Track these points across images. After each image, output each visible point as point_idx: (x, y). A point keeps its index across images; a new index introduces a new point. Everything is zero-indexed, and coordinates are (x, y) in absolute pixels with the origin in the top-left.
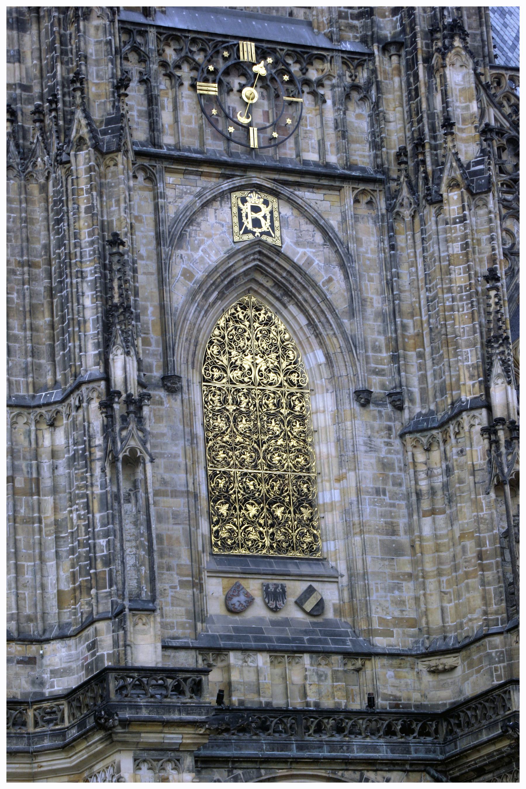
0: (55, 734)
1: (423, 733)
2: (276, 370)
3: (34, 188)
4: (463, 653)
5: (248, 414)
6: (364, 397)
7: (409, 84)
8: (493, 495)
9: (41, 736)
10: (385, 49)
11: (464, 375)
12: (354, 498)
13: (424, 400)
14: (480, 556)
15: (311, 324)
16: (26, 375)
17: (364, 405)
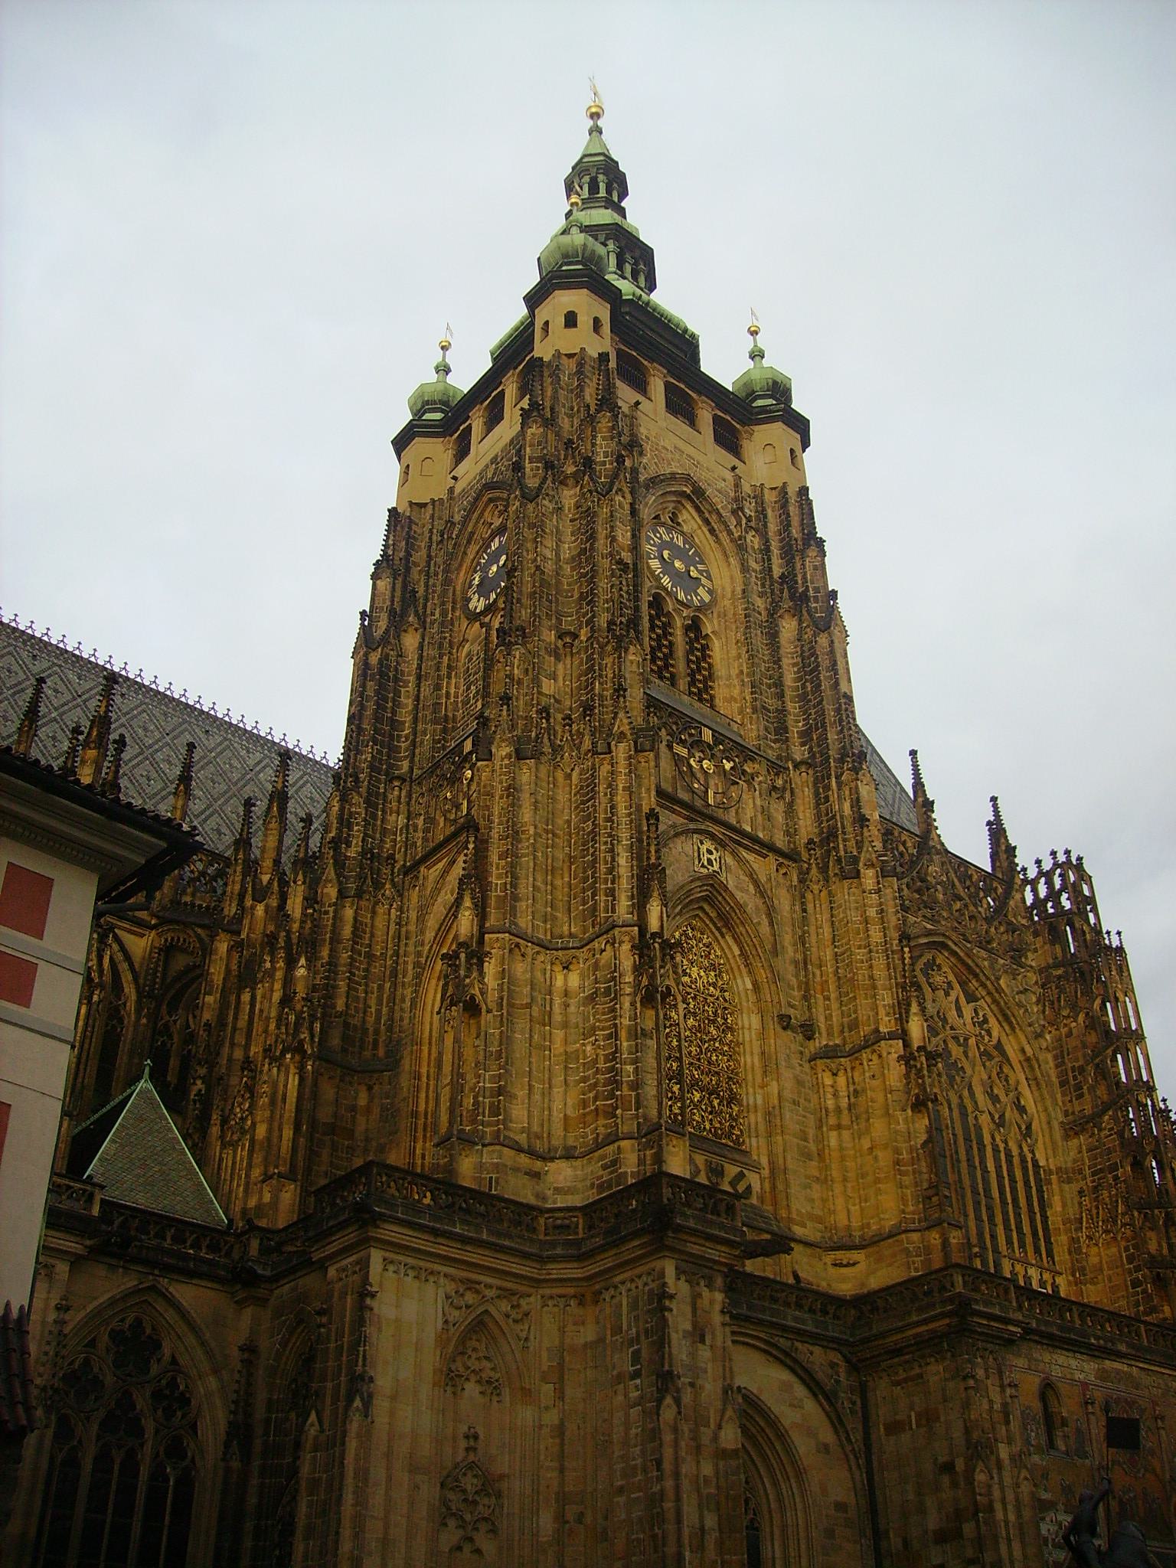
0: (568, 1244)
1: (836, 1317)
2: (714, 985)
3: (560, 775)
4: (870, 1250)
5: (695, 1014)
6: (785, 1022)
7: (817, 794)
8: (909, 1111)
9: (553, 1245)
10: (796, 766)
11: (882, 1012)
12: (776, 1102)
13: (830, 1034)
14: (897, 1163)
15: (743, 954)
16: (545, 922)
17: (784, 1028)
